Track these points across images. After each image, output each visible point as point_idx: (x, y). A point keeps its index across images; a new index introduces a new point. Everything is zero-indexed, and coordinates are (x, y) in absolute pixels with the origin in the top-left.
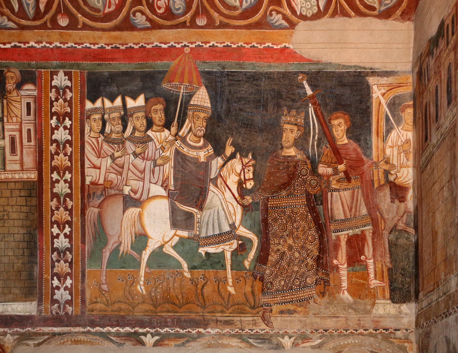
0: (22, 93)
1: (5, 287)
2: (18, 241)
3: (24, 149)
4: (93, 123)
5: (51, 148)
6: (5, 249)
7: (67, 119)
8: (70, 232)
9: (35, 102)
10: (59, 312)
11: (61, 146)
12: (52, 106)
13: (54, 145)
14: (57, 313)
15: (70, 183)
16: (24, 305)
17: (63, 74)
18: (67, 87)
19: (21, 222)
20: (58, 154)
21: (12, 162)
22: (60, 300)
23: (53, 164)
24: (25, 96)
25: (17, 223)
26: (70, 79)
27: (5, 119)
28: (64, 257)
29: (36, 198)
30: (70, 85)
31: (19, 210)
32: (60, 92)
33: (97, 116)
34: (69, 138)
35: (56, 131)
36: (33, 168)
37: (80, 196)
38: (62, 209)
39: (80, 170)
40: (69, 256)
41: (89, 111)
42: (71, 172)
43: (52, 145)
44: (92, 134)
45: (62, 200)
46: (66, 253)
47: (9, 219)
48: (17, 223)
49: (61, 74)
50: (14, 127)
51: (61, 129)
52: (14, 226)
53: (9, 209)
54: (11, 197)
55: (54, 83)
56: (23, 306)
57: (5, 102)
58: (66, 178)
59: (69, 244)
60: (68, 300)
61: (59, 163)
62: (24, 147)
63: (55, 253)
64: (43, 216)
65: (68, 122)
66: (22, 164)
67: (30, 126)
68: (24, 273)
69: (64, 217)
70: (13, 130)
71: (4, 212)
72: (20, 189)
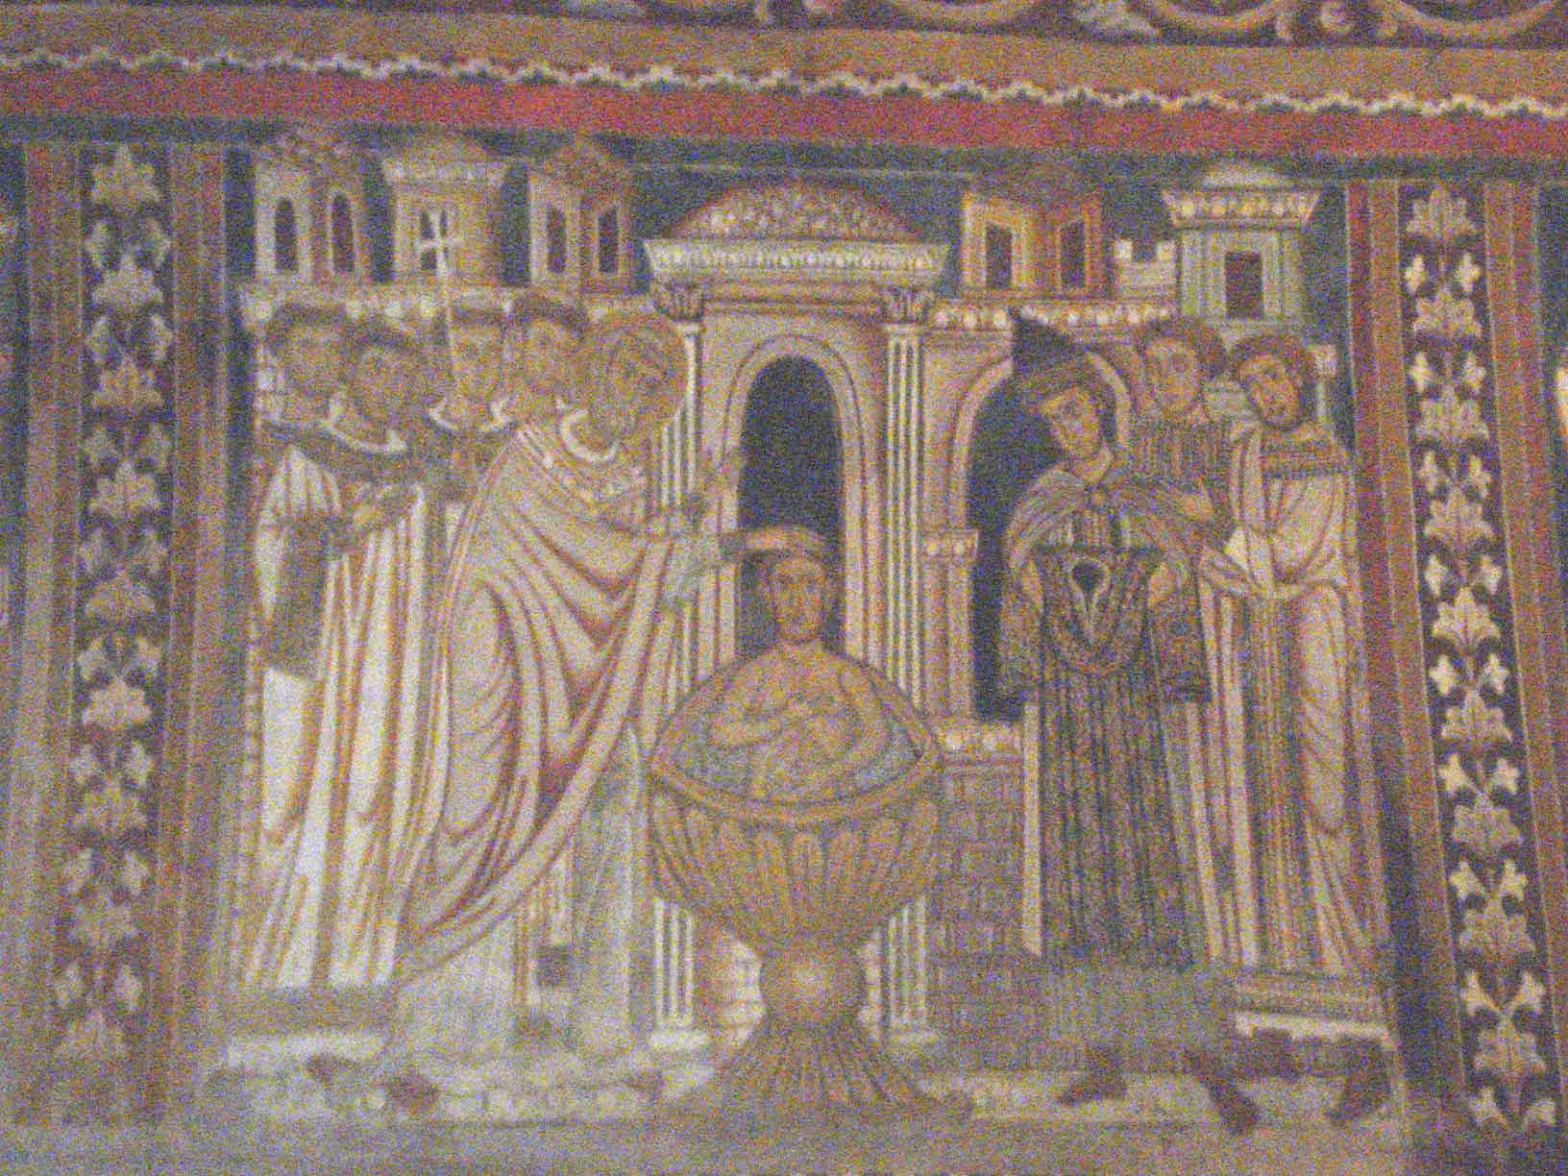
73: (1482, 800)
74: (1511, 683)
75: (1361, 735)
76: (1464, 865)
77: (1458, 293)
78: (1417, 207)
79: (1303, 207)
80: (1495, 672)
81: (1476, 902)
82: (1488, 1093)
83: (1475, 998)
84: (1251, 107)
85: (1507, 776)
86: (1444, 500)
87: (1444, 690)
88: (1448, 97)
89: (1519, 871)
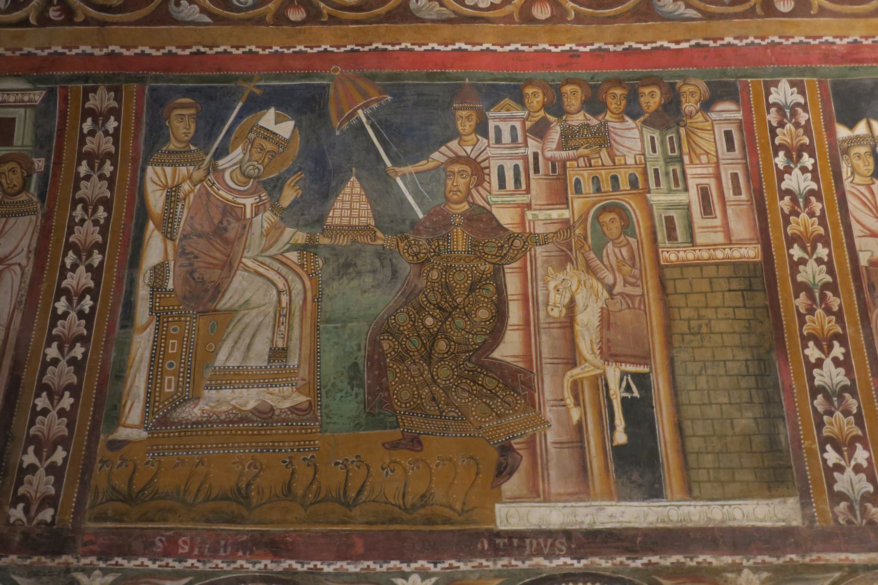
0: (713, 116)
1: (719, 468)
2: (737, 375)
3: (728, 207)
4: (855, 161)
6: (708, 390)
7: (806, 155)
8: (844, 354)
9: (741, 130)
10: (854, 520)
11: (801, 200)
12: (774, 135)
13: (787, 198)
14: (849, 522)
15: (829, 265)
16: (767, 504)
17: (788, 85)
18: (798, 104)
19: (737, 337)
20: (797, 215)
21: (706, 230)
22: (850, 493)
23: (790, 231)
24: (720, 120)
25: (728, 340)
26: (802, 92)
27: (686, 159)
28: (840, 404)
30: (803, 101)
31: (732, 316)
32: (785, 113)
33: (863, 150)
34: (814, 186)
35: (786, 176)
36: (751, 240)
37: (853, 288)
38: (819, 311)
39: (844, 241)
40: (853, 404)
41: (844, 141)
42: (826, 244)
44: (858, 179)
45: (817, 295)
46: (844, 397)
47: (712, 333)
48: (728, 340)
49: (784, 84)
50: (705, 171)
51: (796, 171)
52: (725, 346)
53: (709, 313)
54: (712, 292)
55: (771, 99)
56: (766, 507)
57: (682, 131)
58: (819, 256)
59: (846, 378)
60: (868, 492)
61: (802, 229)
62: (728, 203)
63: (820, 396)
65: (807, 161)
67: (734, 169)
68: (757, 439)
69: (826, 327)
71: (699, 319)
72: (729, 278)
73: (63, 363)
74: (93, 309)
75: (13, 335)
76: (44, 394)
77: (106, 133)
78: (91, 95)
79: (38, 97)
81: (45, 412)
82: (21, 506)
83: (30, 458)
84: (18, 53)
85: (78, 351)
86: (82, 226)
87: (60, 312)
88: (107, 47)
89: (71, 396)
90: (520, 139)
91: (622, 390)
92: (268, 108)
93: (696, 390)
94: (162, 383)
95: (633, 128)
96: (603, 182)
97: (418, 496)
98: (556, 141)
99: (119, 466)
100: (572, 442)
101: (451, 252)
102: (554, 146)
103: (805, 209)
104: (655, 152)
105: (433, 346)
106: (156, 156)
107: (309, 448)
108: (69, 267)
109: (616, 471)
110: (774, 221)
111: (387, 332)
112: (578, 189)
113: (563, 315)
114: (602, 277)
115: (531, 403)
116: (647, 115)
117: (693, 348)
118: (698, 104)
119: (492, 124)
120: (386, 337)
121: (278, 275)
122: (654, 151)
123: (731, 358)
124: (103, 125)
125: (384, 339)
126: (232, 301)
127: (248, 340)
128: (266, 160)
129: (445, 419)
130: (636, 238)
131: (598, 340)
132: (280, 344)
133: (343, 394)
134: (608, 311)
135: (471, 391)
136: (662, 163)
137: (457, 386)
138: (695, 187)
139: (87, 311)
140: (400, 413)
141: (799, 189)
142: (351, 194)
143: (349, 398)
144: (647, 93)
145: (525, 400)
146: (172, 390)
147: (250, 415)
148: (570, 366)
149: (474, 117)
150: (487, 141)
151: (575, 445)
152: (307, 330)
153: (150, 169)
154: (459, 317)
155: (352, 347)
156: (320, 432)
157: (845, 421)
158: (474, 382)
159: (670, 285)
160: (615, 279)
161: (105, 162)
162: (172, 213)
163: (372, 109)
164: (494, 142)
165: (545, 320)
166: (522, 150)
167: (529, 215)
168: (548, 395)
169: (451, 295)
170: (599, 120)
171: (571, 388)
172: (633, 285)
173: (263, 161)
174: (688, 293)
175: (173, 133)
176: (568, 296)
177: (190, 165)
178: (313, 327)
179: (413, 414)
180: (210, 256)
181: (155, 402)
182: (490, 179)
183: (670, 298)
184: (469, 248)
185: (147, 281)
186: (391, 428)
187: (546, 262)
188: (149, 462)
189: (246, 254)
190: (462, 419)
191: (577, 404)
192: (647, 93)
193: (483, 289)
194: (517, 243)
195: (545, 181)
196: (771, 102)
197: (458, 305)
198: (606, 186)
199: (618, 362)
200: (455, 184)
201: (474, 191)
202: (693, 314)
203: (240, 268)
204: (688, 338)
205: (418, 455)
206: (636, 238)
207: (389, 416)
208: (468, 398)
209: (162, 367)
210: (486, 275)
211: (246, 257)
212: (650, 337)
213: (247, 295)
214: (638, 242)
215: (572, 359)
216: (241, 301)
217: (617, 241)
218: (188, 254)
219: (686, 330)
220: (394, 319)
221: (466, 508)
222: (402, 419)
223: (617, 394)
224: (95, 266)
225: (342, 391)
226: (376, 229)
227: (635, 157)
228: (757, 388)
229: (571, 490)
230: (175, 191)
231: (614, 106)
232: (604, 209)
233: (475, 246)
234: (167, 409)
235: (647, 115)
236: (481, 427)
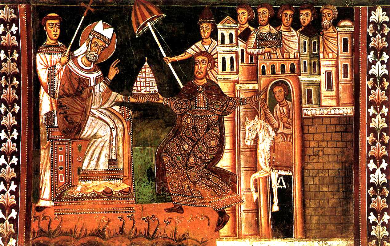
0: (339, 29)
2: (333, 177)
3: (340, 85)
5: (367, 83)
9: (352, 38)
11: (378, 80)
12: (370, 41)
13: (371, 79)
17: (381, 10)
18: (385, 22)
20: (375, 89)
21: (327, 98)
23: (370, 99)
28: (380, 192)
29: (351, 133)
35: (373, 66)
43: (368, 80)
45: (379, 134)
47: (324, 155)
49: (379, 9)
50: (330, 63)
51: (379, 63)
53: (324, 144)
54: (327, 133)
63: (372, 188)
64: (359, 151)
66: (338, 99)
67: (346, 62)
68: (339, 209)
70: (329, 66)
71: (318, 147)
73: (8, 166)
74: (18, 136)
80: (15, 134)
90: (234, 41)
91: (278, 184)
92: (99, 20)
93: (313, 184)
94: (58, 177)
95: (295, 36)
96: (277, 68)
97: (181, 235)
98: (254, 43)
99: (42, 220)
100: (253, 210)
101: (197, 108)
102: (252, 46)
103: (379, 86)
104: (305, 51)
105: (188, 160)
106: (41, 48)
107: (130, 211)
108: (3, 113)
109: (272, 224)
110: (363, 91)
111: (166, 152)
112: (264, 73)
113: (252, 144)
114: (273, 123)
115: (234, 190)
116: (303, 27)
117: (314, 162)
118: (331, 21)
119: (219, 32)
120: (165, 155)
121: (110, 120)
122: (305, 50)
123: (332, 168)
124: (10, 29)
125: (164, 156)
126: (88, 134)
127: (97, 155)
128: (99, 52)
129: (194, 197)
130: (292, 102)
131: (268, 158)
132: (113, 157)
133: (145, 184)
134: (274, 142)
135: (206, 183)
136: (308, 58)
137: (199, 181)
138: (324, 72)
139: (16, 138)
140: (172, 194)
141: (378, 74)
142: (145, 73)
143: (148, 186)
144: (304, 14)
145: (232, 189)
146: (63, 181)
147: (102, 194)
148: (254, 172)
149: (210, 28)
150: (217, 42)
151: (253, 211)
152: (126, 150)
153: (38, 55)
154: (201, 145)
155: (148, 160)
156: (135, 203)
157: (381, 200)
158: (208, 179)
159: (306, 128)
160: (279, 125)
161: (13, 52)
162: (53, 82)
163: (155, 22)
164: (220, 43)
165: (243, 147)
166: (234, 49)
167: (238, 86)
168: (243, 186)
169: (197, 133)
170: (277, 30)
171: (254, 183)
172: (288, 128)
173: (98, 52)
174: (315, 133)
175: (48, 35)
176: (255, 134)
177: (59, 54)
178: (129, 148)
179: (179, 195)
180: (74, 108)
181: (56, 187)
182: (218, 65)
183: (305, 135)
184: (206, 106)
185: (44, 122)
186: (169, 201)
187: (245, 114)
188: (56, 217)
189: (93, 107)
190: (202, 198)
191: (256, 191)
192: (304, 14)
193: (213, 129)
194: (231, 103)
195: (246, 67)
196: (370, 21)
197: (201, 138)
198: (278, 71)
199: (277, 170)
200: (199, 68)
201: (209, 72)
202: (316, 145)
203: (90, 115)
204: (312, 157)
205: (181, 215)
206: (292, 102)
207: (168, 196)
208: (205, 187)
209: (57, 169)
210: (215, 121)
211: (93, 109)
212: (294, 156)
213: (95, 131)
214: (292, 104)
215: (255, 168)
216: (92, 134)
217: (281, 103)
218: (64, 106)
219: (311, 153)
220: (169, 145)
221: (203, 240)
222: (174, 197)
223: (275, 186)
224: (17, 112)
225: (145, 182)
226: (159, 94)
227: (295, 54)
228: (342, 184)
229: (251, 233)
230: (53, 69)
231: (286, 21)
232: (276, 84)
233: (210, 105)
234: (62, 191)
235: (303, 27)
236: (210, 202)
